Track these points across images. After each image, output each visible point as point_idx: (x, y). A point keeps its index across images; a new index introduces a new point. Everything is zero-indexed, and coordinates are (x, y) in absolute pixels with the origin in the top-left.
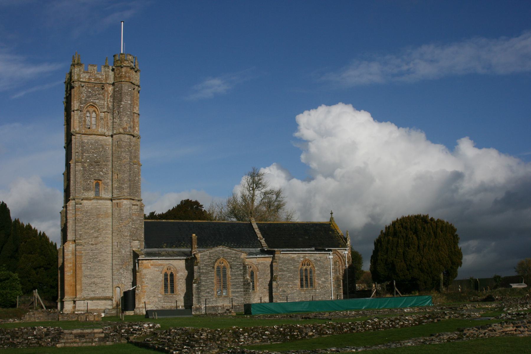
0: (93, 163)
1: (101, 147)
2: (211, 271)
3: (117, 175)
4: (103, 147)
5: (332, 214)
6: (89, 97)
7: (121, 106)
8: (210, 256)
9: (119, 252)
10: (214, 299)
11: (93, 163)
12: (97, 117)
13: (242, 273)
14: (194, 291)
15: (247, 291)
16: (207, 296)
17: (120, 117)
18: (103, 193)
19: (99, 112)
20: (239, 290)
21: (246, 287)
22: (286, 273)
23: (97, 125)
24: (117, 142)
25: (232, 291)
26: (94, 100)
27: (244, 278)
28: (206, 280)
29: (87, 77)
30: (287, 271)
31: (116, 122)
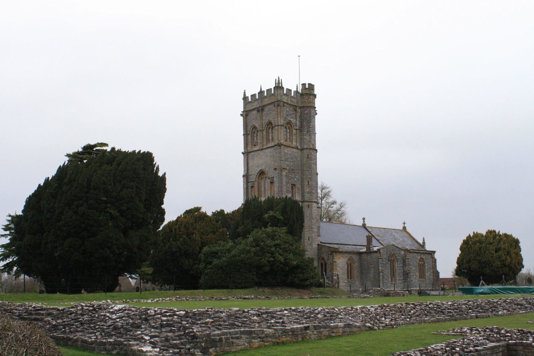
0: (291, 171)
1: (295, 157)
2: (388, 263)
3: (308, 182)
4: (296, 158)
5: (404, 223)
6: (287, 115)
7: (311, 126)
8: (387, 252)
9: (311, 245)
10: (389, 285)
11: (291, 171)
12: (291, 133)
13: (401, 265)
14: (381, 278)
15: (406, 279)
16: (386, 282)
17: (310, 135)
18: (296, 196)
19: (293, 129)
20: (401, 278)
21: (406, 276)
22: (412, 267)
23: (291, 139)
24: (308, 155)
25: (398, 279)
26: (290, 118)
27: (404, 269)
28: (385, 270)
29: (286, 99)
30: (413, 266)
31: (306, 139)
